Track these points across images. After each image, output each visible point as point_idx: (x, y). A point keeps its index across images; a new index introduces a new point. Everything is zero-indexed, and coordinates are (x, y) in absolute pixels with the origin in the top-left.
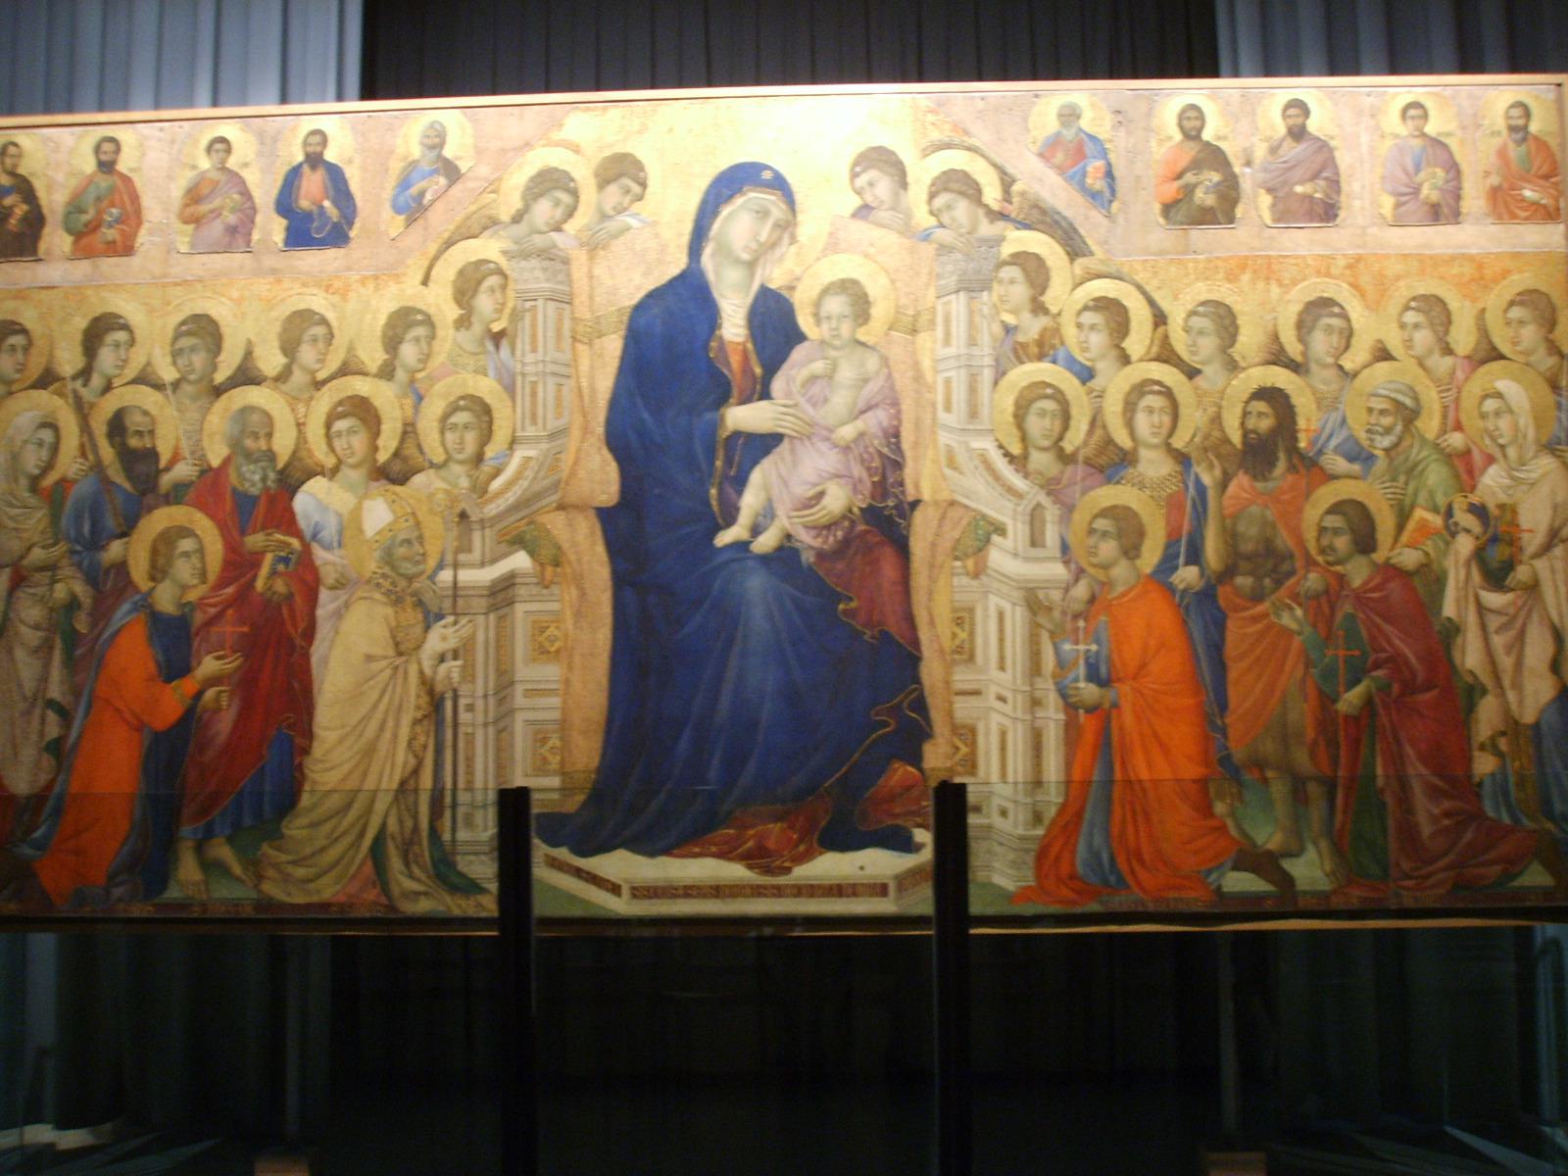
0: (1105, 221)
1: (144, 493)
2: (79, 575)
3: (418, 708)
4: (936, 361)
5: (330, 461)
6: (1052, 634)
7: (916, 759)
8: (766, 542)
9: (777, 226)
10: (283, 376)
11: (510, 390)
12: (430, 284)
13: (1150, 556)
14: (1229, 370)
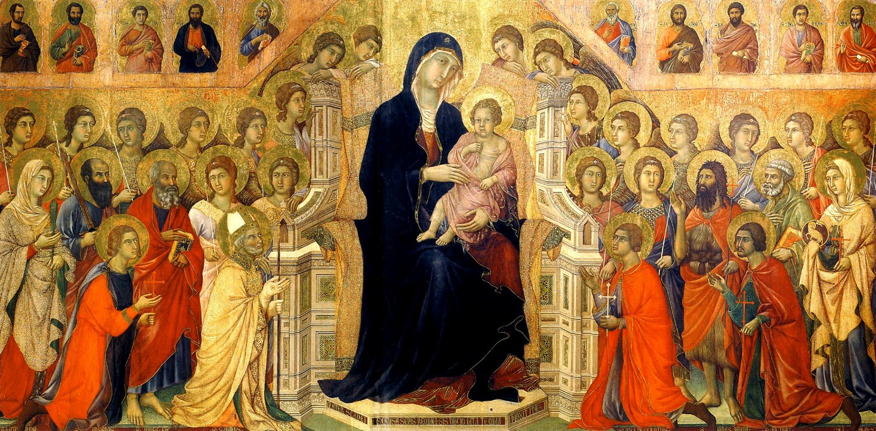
8: (444, 240)
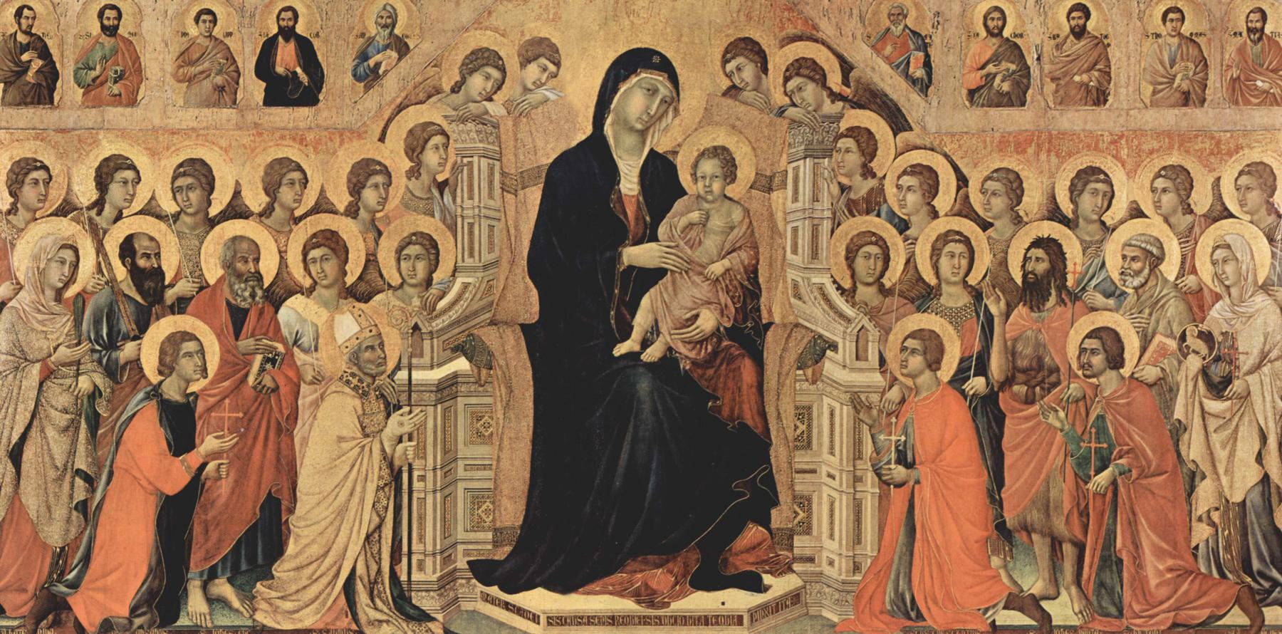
0: (923, 104)
1: (152, 305)
2: (100, 370)
3: (380, 478)
5: (307, 283)
6: (871, 427)
7: (765, 522)
8: (653, 354)
9: (663, 101)
10: (267, 212)
11: (453, 229)
12: (386, 140)
14: (1015, 224)
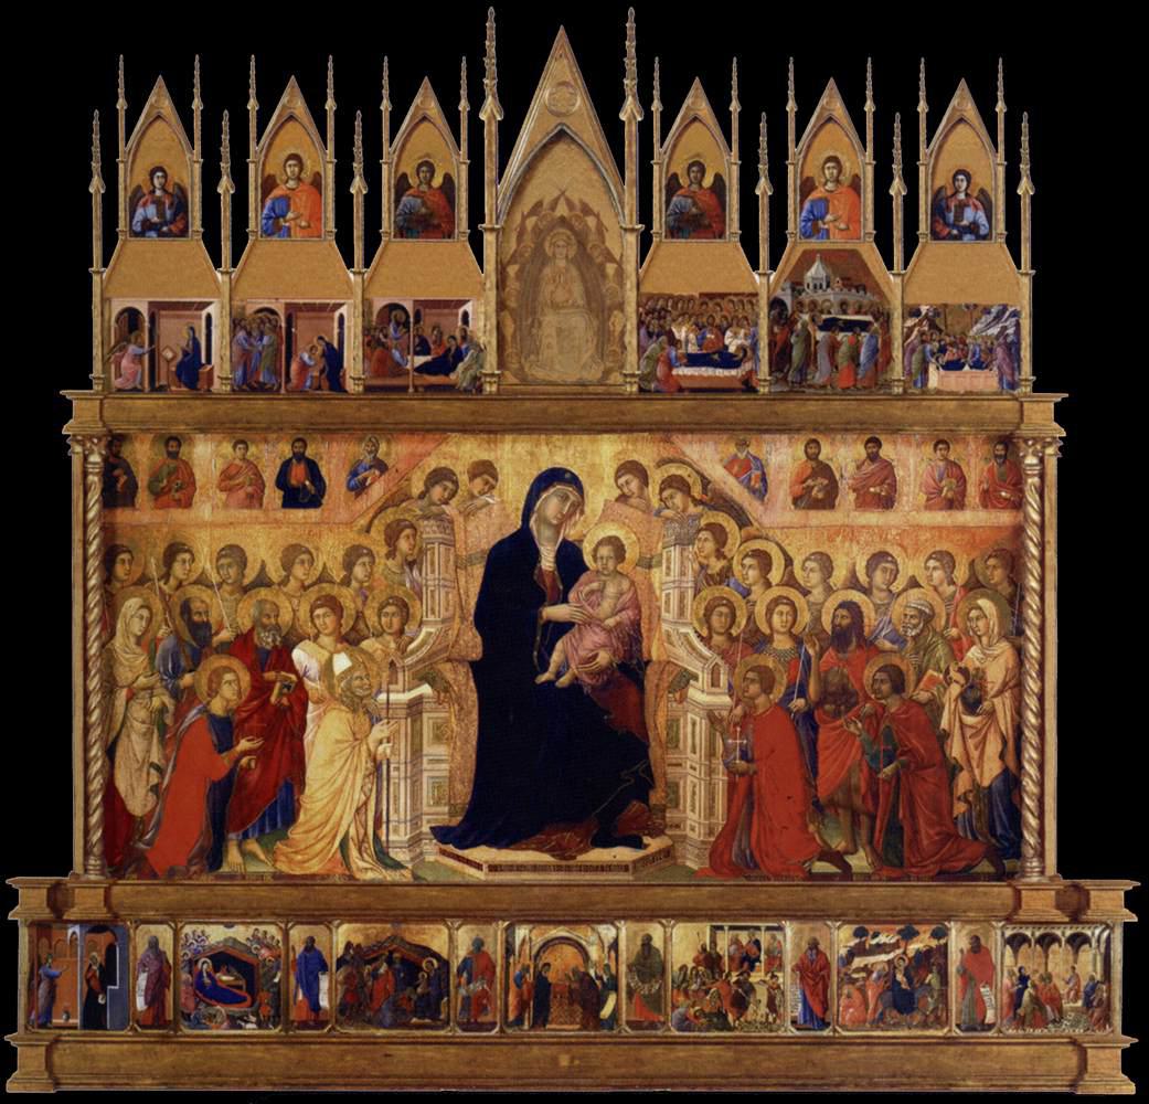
4: (662, 584)
8: (564, 681)
9: (573, 504)
13: (778, 693)
